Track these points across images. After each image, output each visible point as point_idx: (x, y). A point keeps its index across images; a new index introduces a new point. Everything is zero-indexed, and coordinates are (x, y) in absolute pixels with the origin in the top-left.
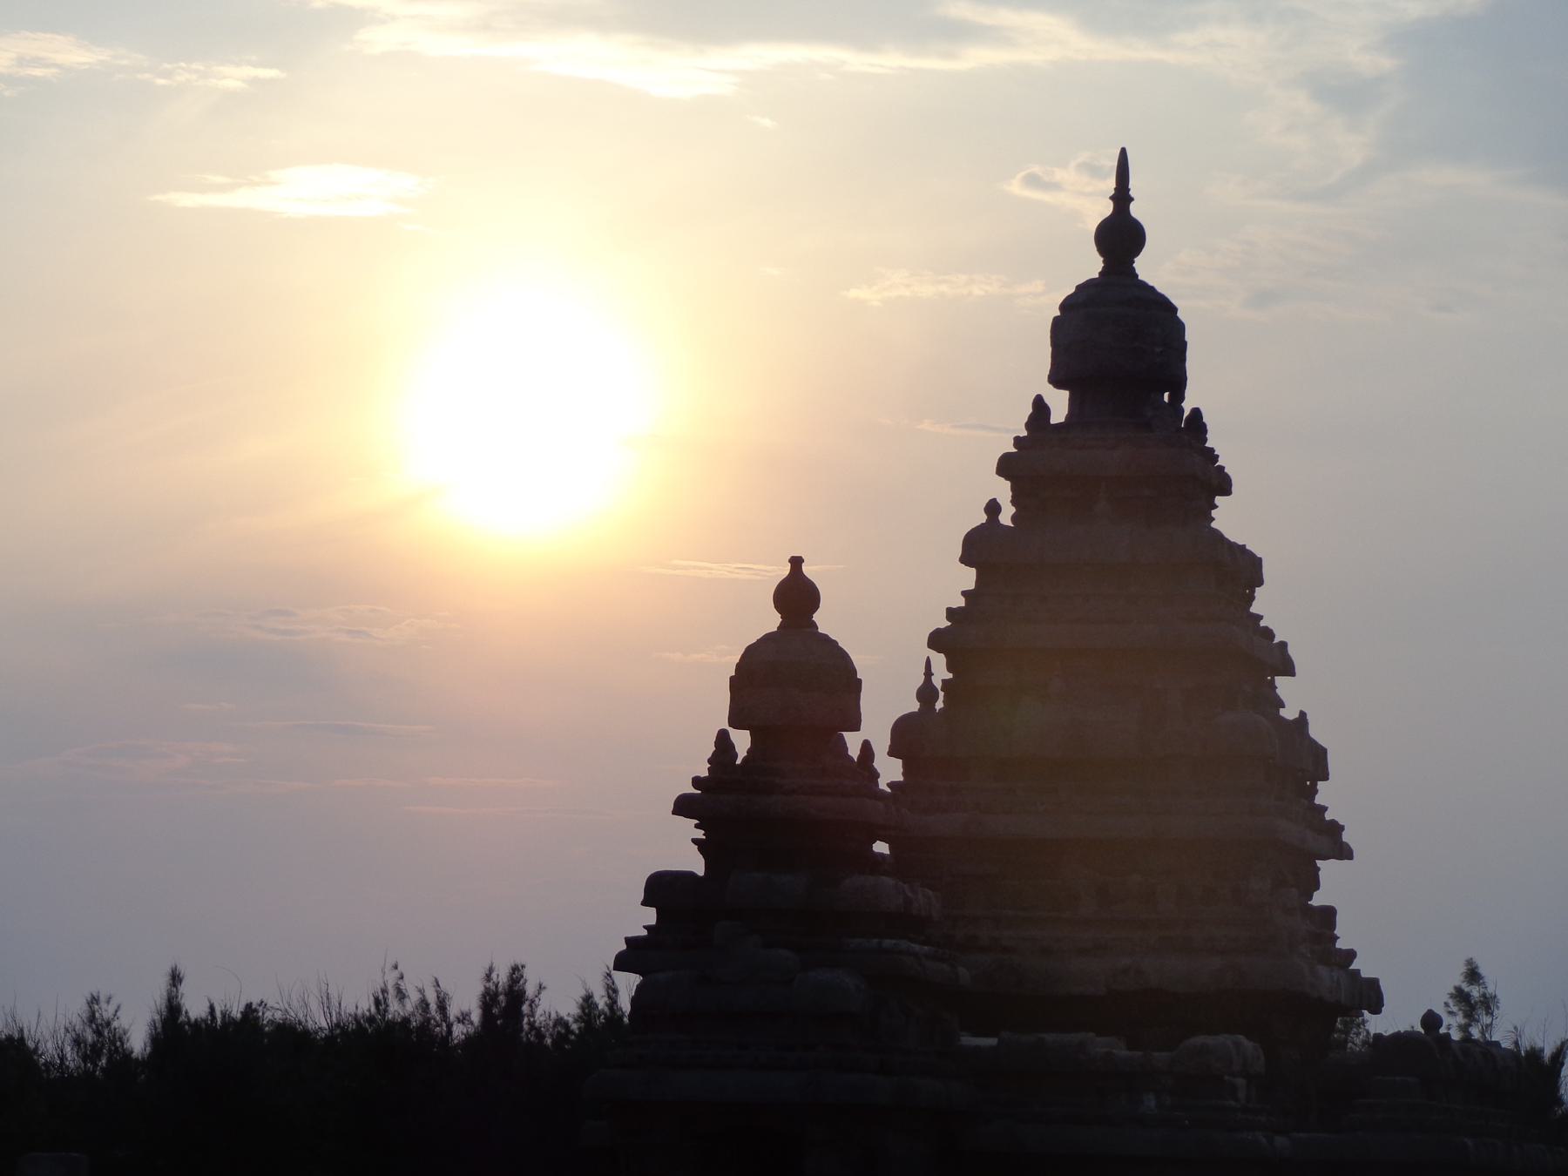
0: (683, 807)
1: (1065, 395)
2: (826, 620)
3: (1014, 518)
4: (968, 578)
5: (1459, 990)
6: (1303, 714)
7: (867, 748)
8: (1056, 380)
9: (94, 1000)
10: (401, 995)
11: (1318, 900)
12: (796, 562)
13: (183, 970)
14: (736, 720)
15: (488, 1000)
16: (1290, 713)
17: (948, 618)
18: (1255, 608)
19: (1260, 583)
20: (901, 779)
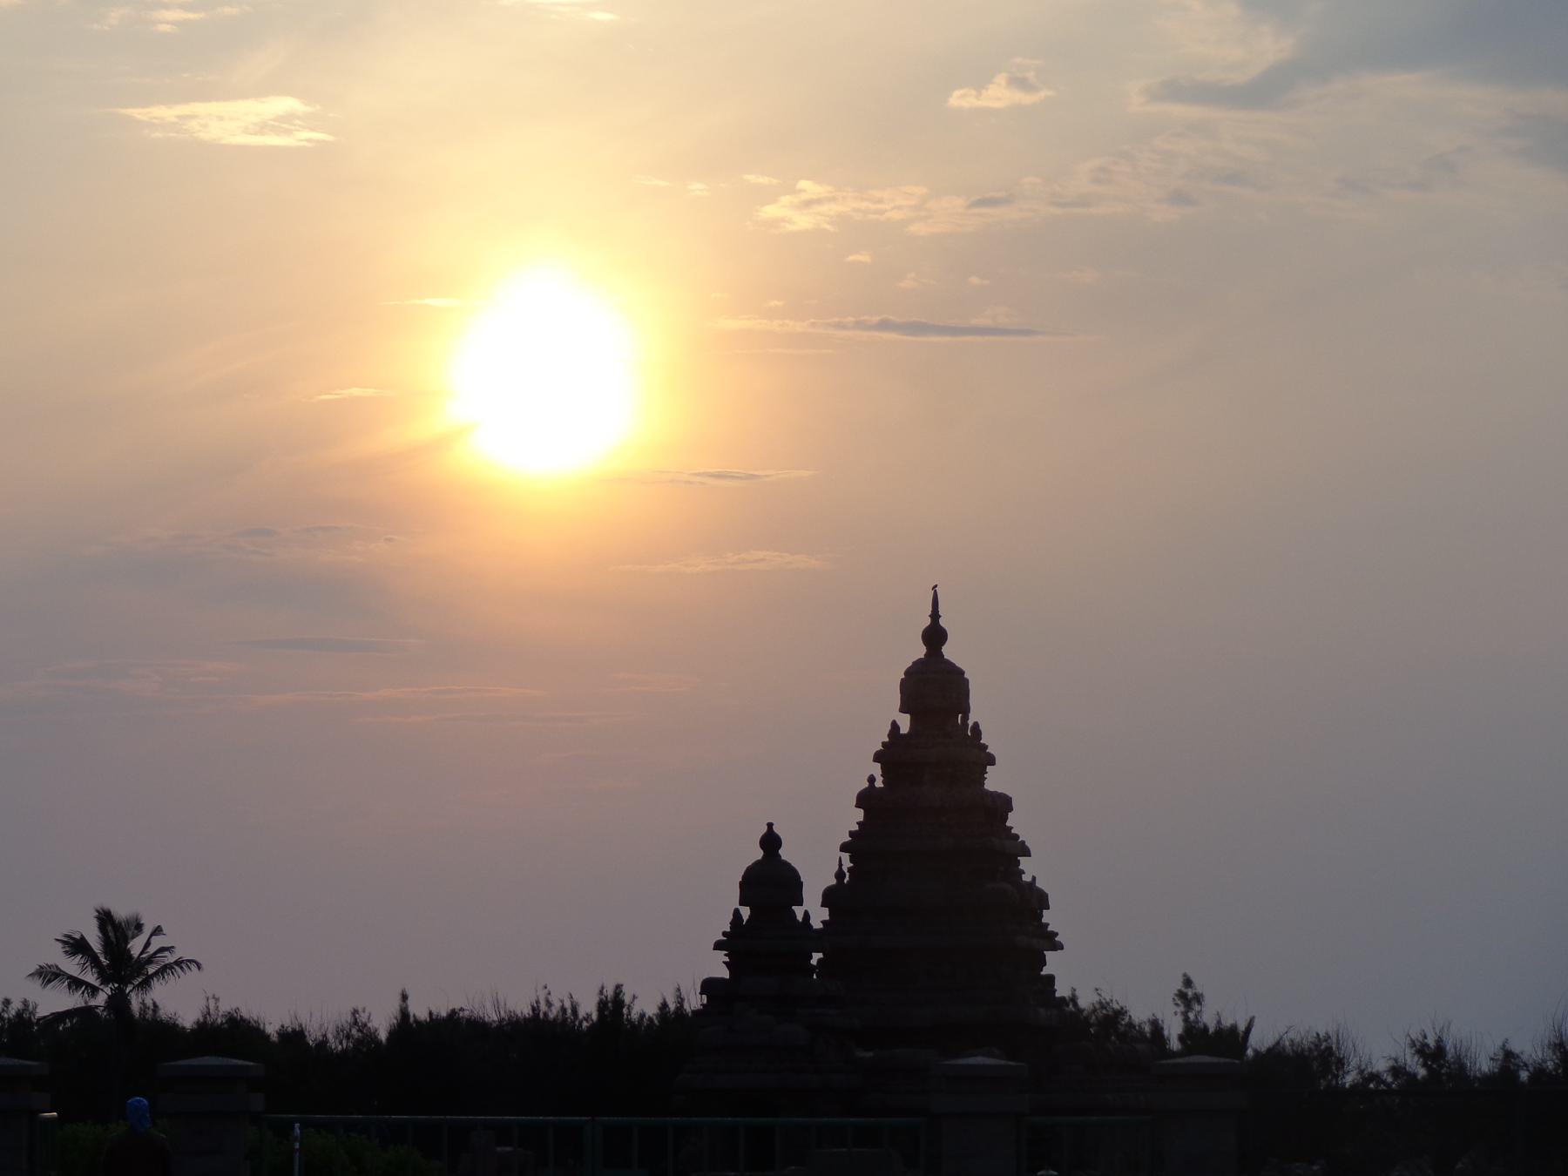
0: (718, 946)
1: (908, 717)
2: (785, 853)
3: (883, 782)
4: (860, 815)
5: (1180, 991)
6: (1034, 878)
7: (807, 915)
8: (902, 710)
9: (355, 1012)
10: (549, 1004)
11: (1045, 971)
12: (770, 826)
13: (409, 992)
14: (741, 904)
15: (602, 1005)
16: (1026, 878)
17: (850, 836)
18: (1008, 824)
19: (1011, 810)
20: (828, 918)
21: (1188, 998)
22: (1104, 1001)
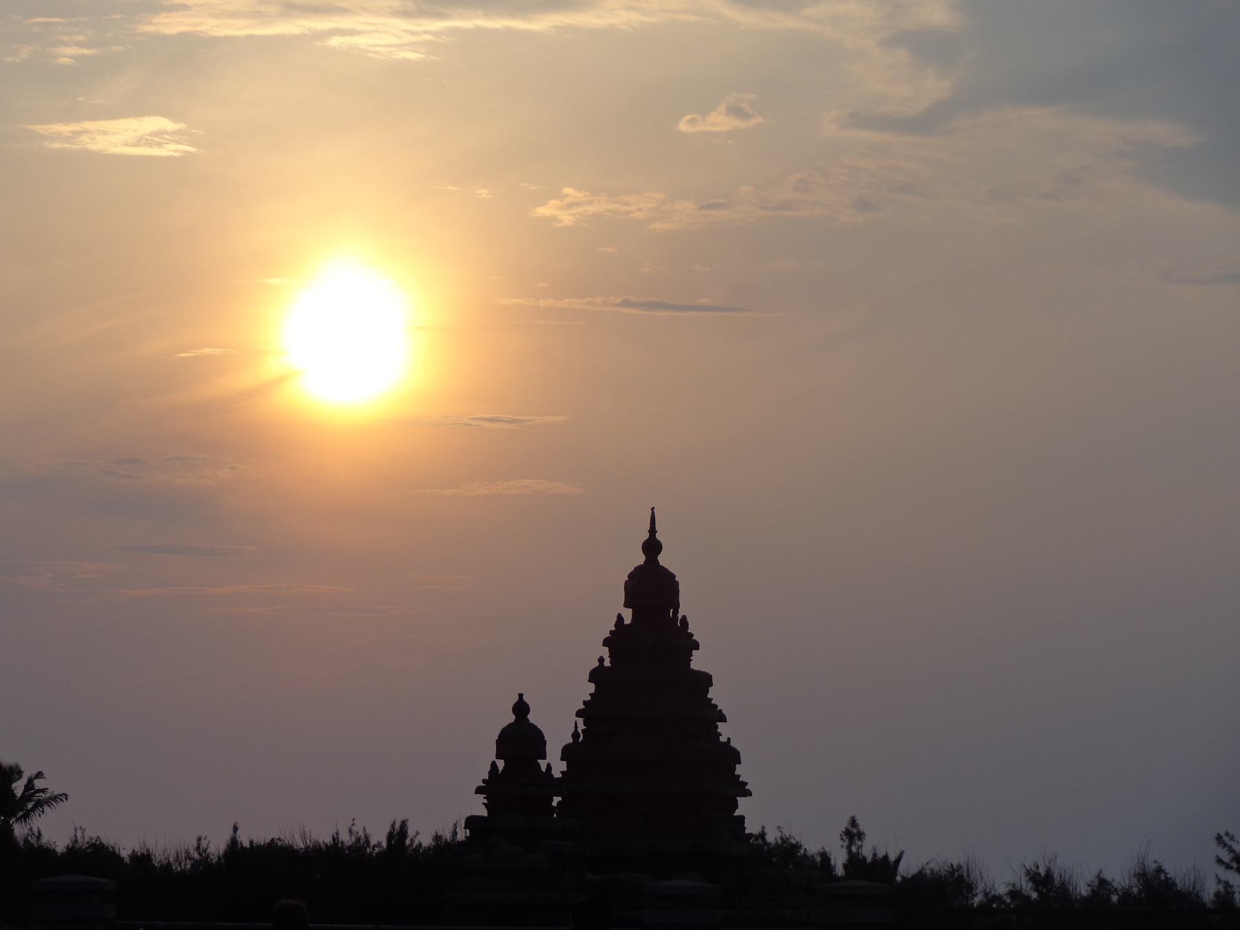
0: (479, 791)
1: (630, 611)
2: (532, 718)
3: (610, 663)
4: (591, 688)
6: (729, 739)
7: (549, 767)
11: (737, 813)
12: (521, 696)
13: (238, 825)
14: (497, 758)
15: (390, 836)
16: (723, 739)
17: (584, 704)
19: (711, 685)
20: (566, 769)
21: (853, 834)
22: (784, 837)
